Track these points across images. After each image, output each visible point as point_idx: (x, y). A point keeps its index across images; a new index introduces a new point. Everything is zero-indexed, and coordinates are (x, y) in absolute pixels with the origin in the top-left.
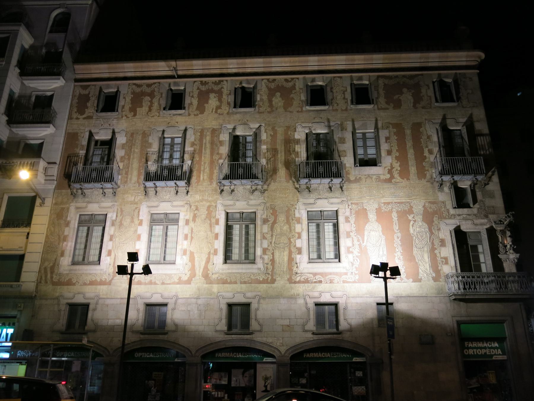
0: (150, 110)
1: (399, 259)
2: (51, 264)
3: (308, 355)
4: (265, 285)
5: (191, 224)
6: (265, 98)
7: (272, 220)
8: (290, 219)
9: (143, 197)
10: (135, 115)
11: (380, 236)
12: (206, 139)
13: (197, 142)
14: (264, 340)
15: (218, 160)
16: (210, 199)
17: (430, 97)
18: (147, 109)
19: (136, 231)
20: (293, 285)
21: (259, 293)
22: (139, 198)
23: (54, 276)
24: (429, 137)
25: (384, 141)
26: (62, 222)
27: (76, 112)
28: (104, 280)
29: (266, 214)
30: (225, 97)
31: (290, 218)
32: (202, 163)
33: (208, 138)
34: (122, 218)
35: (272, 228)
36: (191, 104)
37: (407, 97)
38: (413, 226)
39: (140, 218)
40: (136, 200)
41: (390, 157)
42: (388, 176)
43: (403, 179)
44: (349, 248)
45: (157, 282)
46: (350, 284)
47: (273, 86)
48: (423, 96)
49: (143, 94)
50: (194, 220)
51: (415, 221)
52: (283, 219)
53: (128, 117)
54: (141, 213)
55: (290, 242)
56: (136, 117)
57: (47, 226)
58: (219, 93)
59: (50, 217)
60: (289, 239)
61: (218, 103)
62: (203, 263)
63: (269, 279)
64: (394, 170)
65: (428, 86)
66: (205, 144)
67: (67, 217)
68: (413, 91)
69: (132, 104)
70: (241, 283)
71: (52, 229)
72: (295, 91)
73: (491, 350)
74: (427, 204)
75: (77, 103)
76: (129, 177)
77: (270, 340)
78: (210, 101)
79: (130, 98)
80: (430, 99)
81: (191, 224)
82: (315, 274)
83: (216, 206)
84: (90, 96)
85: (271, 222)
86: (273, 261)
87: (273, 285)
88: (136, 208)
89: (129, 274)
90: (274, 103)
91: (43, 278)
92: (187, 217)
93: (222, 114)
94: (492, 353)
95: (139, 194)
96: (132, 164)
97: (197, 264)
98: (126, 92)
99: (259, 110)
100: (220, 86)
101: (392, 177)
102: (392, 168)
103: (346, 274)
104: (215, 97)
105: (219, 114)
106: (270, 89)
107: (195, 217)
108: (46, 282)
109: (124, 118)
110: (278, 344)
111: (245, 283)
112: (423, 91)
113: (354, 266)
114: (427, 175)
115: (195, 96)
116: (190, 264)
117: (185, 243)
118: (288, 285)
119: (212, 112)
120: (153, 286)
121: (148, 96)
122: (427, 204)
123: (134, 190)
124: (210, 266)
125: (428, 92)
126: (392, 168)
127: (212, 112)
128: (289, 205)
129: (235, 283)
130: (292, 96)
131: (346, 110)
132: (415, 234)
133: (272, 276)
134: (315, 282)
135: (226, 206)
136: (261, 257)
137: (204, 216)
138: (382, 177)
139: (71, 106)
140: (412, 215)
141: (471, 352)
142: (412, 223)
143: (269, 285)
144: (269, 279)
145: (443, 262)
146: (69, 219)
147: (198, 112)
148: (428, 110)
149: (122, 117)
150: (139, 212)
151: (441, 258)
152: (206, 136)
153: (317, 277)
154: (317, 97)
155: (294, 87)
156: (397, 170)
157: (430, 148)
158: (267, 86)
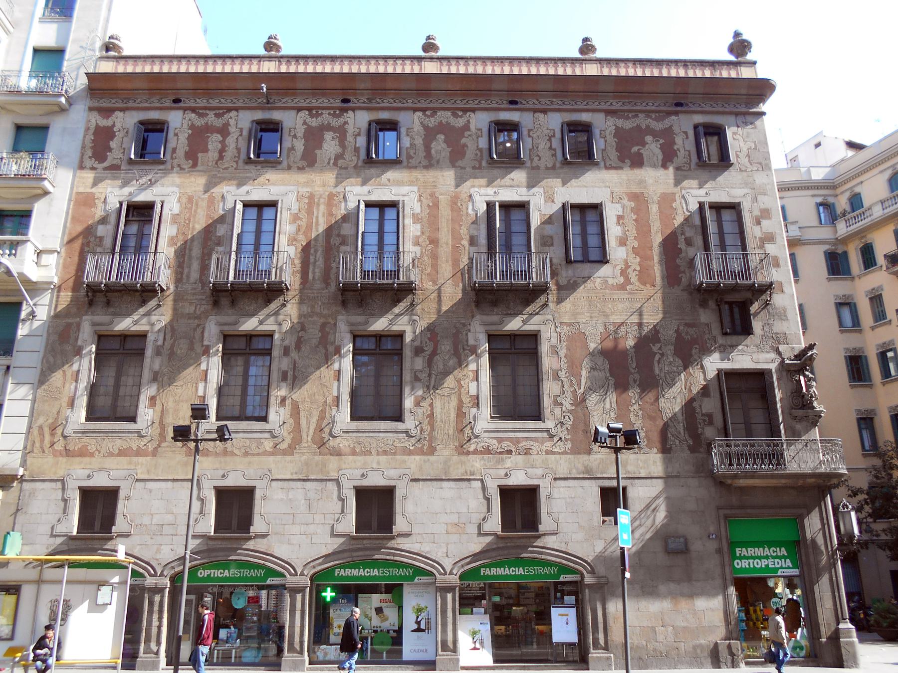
0: (221, 157)
1: (637, 416)
2: (50, 421)
3: (488, 572)
4: (418, 458)
5: (294, 354)
6: (419, 141)
7: (429, 349)
9: (210, 307)
10: (195, 165)
11: (607, 378)
12: (318, 210)
13: (303, 215)
14: (415, 548)
15: (338, 247)
16: (325, 312)
17: (689, 151)
18: (216, 155)
20: (463, 458)
21: (407, 472)
22: (202, 309)
25: (615, 220)
26: (69, 348)
27: (90, 157)
29: (419, 340)
30: (350, 138)
31: (460, 347)
32: (312, 251)
33: (322, 208)
34: (175, 341)
35: (430, 363)
36: (292, 148)
38: (659, 362)
39: (206, 343)
40: (198, 312)
41: (624, 249)
43: (644, 284)
44: (556, 397)
45: (237, 452)
46: (558, 456)
47: (432, 122)
48: (678, 149)
49: (210, 128)
50: (298, 347)
51: (662, 355)
52: (448, 348)
53: (182, 169)
54: (206, 334)
55: (461, 386)
56: (198, 168)
57: (41, 354)
58: (341, 133)
59: (48, 339)
61: (339, 150)
63: (425, 447)
64: (629, 270)
65: (686, 133)
66: (317, 217)
67: (77, 339)
68: (662, 141)
69: (189, 145)
71: (51, 359)
72: (469, 133)
73: (776, 561)
74: (681, 328)
75: (93, 141)
76: (186, 271)
77: (425, 548)
78: (325, 146)
79: (187, 135)
80: (689, 155)
81: (294, 354)
82: (500, 440)
83: (335, 325)
84: (115, 129)
85: (428, 353)
86: (431, 416)
87: (432, 458)
88: (198, 325)
89: (194, 441)
90: (433, 151)
91: (37, 445)
92: (287, 343)
93: (346, 168)
94: (777, 566)
95: (204, 302)
96: (190, 250)
97: (303, 422)
98: (178, 125)
99: (409, 162)
100: (342, 120)
101: (628, 281)
102: (627, 266)
104: (333, 138)
105: (341, 168)
106: (426, 128)
108: (43, 452)
110: (440, 554)
111: (385, 453)
112: (679, 140)
113: (565, 427)
114: (683, 280)
115: (298, 135)
116: (291, 421)
118: (456, 458)
119: (329, 163)
120: (228, 458)
121: (218, 133)
122: (681, 328)
123: (194, 294)
125: (684, 144)
126: (627, 266)
127: (329, 163)
128: (458, 325)
129: (369, 453)
130: (463, 141)
131: (554, 168)
132: (663, 375)
133: (431, 441)
134: (501, 453)
135: (352, 324)
137: (315, 342)
139: (83, 147)
140: (658, 345)
141: (744, 564)
142: (657, 357)
143: (426, 458)
144: (425, 447)
145: (704, 421)
146: (80, 343)
147: (305, 163)
148: (686, 173)
149: (173, 168)
150: (203, 333)
151: (703, 415)
152: (318, 205)
153: (504, 444)
155: (467, 127)
156: (635, 270)
157: (688, 234)
158: (421, 123)
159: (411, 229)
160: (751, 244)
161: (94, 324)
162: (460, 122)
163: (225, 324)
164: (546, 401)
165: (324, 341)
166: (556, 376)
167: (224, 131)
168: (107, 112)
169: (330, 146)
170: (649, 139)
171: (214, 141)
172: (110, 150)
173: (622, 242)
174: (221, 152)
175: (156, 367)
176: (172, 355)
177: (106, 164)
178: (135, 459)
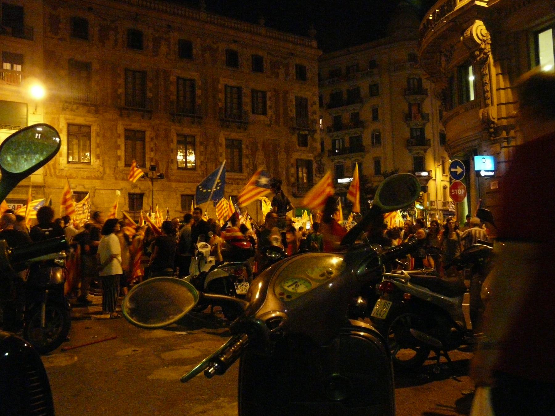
5: (155, 141)
8: (216, 144)
19: (116, 142)
23: (57, 172)
24: (291, 101)
28: (96, 176)
33: (162, 77)
35: (206, 148)
37: (282, 71)
42: (269, 123)
53: (98, 47)
54: (118, 129)
62: (165, 168)
70: (189, 182)
81: (155, 141)
91: (48, 172)
92: (152, 136)
101: (271, 124)
107: (157, 136)
108: (51, 176)
111: (191, 182)
112: (290, 69)
117: (152, 153)
124: (169, 171)
125: (293, 71)
129: (185, 182)
136: (200, 167)
138: (266, 123)
150: (117, 128)
154: (232, 60)
159: (199, 92)
161: (66, 119)
162: (215, 46)
163: (126, 125)
165: (167, 137)
166: (247, 157)
169: (164, 48)
170: (281, 67)
173: (271, 107)
174: (116, 41)
176: (104, 136)
178: (94, 181)
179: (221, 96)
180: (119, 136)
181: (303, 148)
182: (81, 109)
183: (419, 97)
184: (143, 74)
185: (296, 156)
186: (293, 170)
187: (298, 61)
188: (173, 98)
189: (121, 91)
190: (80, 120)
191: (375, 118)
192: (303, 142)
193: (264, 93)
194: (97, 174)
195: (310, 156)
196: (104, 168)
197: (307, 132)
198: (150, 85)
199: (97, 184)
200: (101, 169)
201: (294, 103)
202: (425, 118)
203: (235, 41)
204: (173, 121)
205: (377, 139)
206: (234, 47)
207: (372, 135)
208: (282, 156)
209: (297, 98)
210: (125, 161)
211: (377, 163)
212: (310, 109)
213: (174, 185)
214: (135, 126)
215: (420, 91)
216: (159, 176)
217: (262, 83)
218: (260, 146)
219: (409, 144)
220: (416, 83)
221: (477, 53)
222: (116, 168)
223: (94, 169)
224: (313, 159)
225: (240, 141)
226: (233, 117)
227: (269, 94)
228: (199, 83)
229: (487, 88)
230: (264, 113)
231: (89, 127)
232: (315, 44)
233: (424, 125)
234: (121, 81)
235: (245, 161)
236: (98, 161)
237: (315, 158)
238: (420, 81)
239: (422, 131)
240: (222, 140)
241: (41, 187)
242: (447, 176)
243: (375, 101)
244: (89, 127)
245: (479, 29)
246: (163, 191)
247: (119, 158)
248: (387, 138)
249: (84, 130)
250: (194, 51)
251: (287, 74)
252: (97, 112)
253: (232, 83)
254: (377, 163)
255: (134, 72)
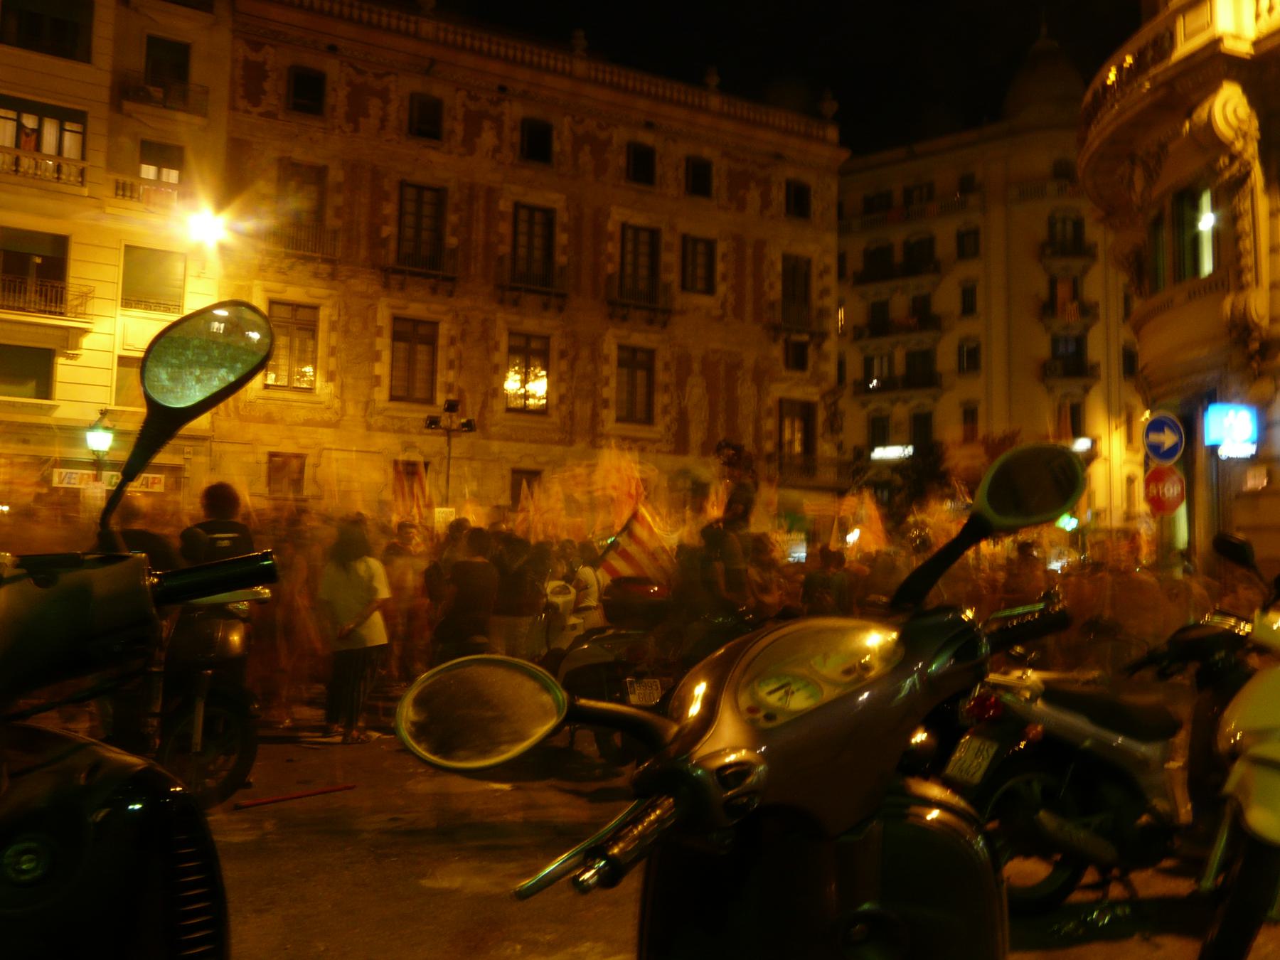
5: (459, 345)
8: (597, 356)
10: (356, 130)
19: (372, 345)
35: (572, 367)
37: (754, 196)
42: (718, 312)
45: (413, 430)
54: (379, 316)
58: (498, 123)
60: (594, 385)
81: (459, 345)
84: (267, 67)
86: (571, 414)
92: (453, 333)
103: (660, 441)
107: (464, 335)
109: (337, 131)
125: (778, 196)
129: (522, 440)
154: (641, 166)
159: (562, 238)
160: (814, 295)
161: (267, 290)
162: (603, 135)
163: (399, 308)
164: (658, 409)
166: (666, 388)
167: (384, 95)
168: (256, 46)
169: (488, 138)
171: (374, 105)
172: (264, 93)
174: (383, 120)
175: (333, 342)
176: (346, 332)
177: (260, 110)
178: (320, 430)
179: (612, 248)
180: (379, 333)
181: (797, 375)
182: (300, 268)
183: (1076, 264)
184: (440, 194)
185: (778, 391)
186: (769, 424)
187: (791, 173)
188: (505, 249)
189: (388, 230)
190: (294, 294)
191: (968, 307)
192: (797, 359)
193: (710, 245)
194: (327, 416)
195: (810, 393)
196: (343, 402)
197: (805, 338)
198: (452, 218)
199: (326, 436)
200: (337, 404)
201: (779, 267)
202: (1088, 311)
203: (649, 126)
204: (501, 302)
205: (970, 359)
206: (647, 138)
207: (960, 348)
208: (746, 390)
209: (786, 258)
210: (391, 388)
211: (970, 415)
212: (816, 285)
213: (496, 446)
214: (416, 309)
215: (1077, 247)
216: (463, 425)
217: (708, 221)
218: (696, 366)
219: (1046, 372)
220: (1069, 228)
221: (1223, 161)
222: (368, 403)
223: (321, 403)
224: (816, 398)
225: (651, 353)
226: (639, 297)
227: (721, 248)
228: (563, 217)
229: (1247, 244)
230: (710, 290)
231: (315, 308)
232: (832, 133)
233: (1087, 328)
234: (389, 209)
235: (661, 400)
236: (331, 385)
237: (823, 397)
238: (1079, 225)
239: (1081, 342)
240: (610, 348)
241: (203, 439)
242: (1137, 451)
243: (969, 269)
244: (315, 308)
245: (1229, 107)
246: (471, 459)
247: (377, 380)
248: (994, 357)
249: (303, 315)
250: (556, 147)
251: (766, 203)
252: (333, 276)
253: (639, 219)
254: (970, 415)
255: (420, 188)
